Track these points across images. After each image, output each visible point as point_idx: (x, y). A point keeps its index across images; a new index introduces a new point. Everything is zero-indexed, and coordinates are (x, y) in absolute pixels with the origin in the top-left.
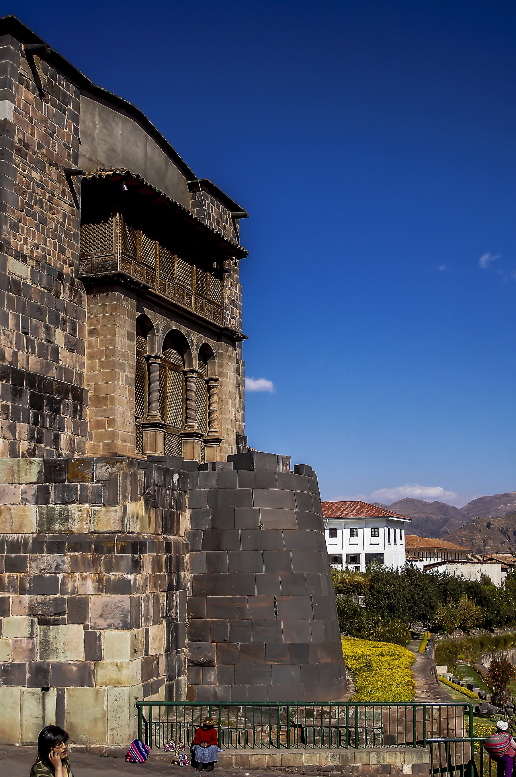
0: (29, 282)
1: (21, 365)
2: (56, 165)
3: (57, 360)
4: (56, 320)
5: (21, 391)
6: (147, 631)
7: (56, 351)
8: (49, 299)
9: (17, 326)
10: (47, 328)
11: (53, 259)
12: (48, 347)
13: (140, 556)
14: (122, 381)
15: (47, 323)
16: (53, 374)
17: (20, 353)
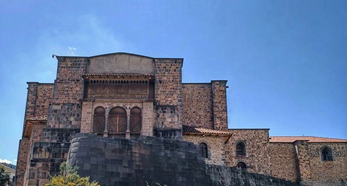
0: (61, 109)
1: (57, 126)
2: (74, 81)
3: (71, 124)
4: (71, 115)
5: (54, 133)
6: (38, 181)
7: (71, 122)
8: (68, 111)
9: (55, 119)
10: (67, 118)
11: (72, 101)
12: (67, 122)
13: (36, 163)
14: (84, 124)
15: (67, 116)
16: (70, 127)
17: (56, 125)
